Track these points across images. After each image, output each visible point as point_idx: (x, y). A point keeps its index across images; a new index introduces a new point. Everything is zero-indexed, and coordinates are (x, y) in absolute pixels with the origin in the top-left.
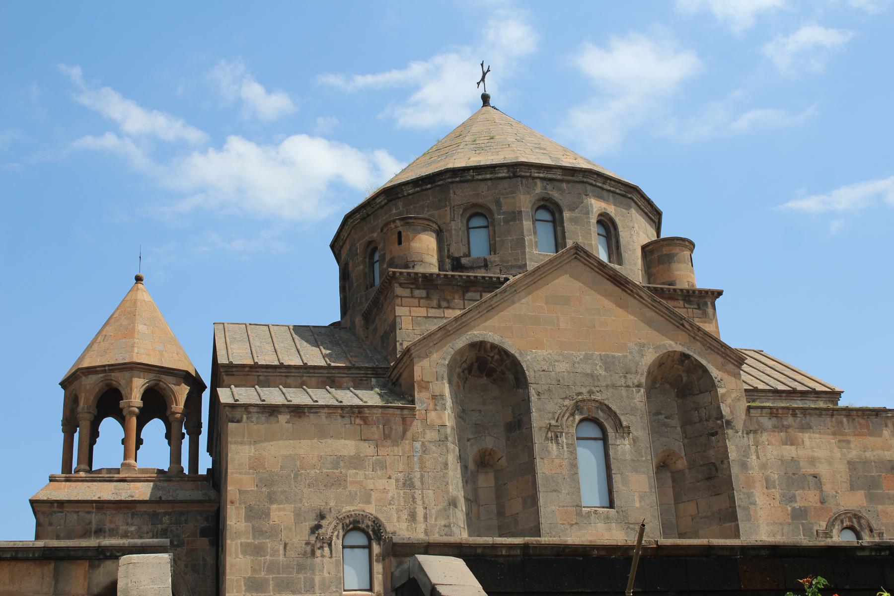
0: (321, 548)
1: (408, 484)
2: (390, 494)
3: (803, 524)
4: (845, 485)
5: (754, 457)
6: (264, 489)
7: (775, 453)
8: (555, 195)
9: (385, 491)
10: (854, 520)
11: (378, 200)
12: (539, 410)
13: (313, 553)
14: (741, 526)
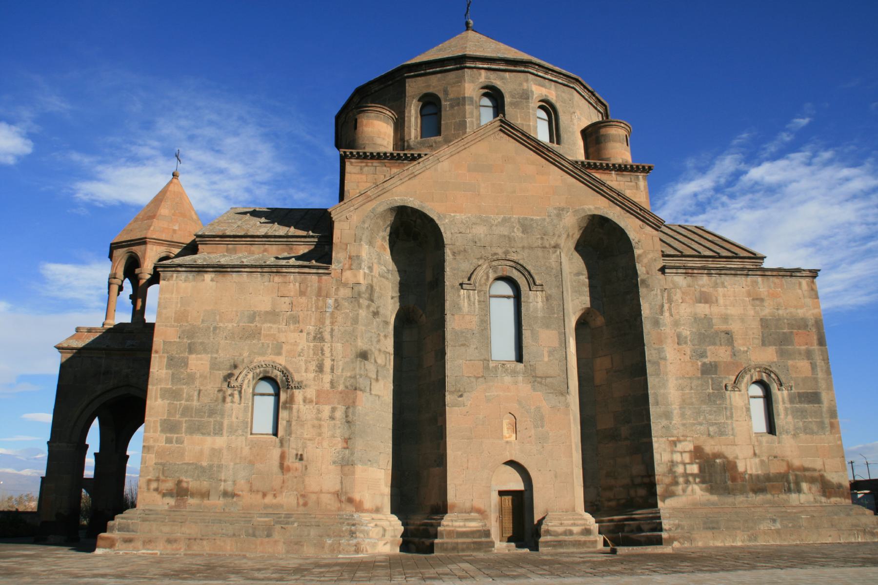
0: (232, 395)
1: (319, 337)
2: (299, 348)
4: (756, 341)
6: (185, 340)
7: (689, 310)
8: (498, 84)
9: (296, 344)
10: (764, 375)
11: (355, 100)
12: (453, 269)
13: (224, 400)
14: (651, 381)
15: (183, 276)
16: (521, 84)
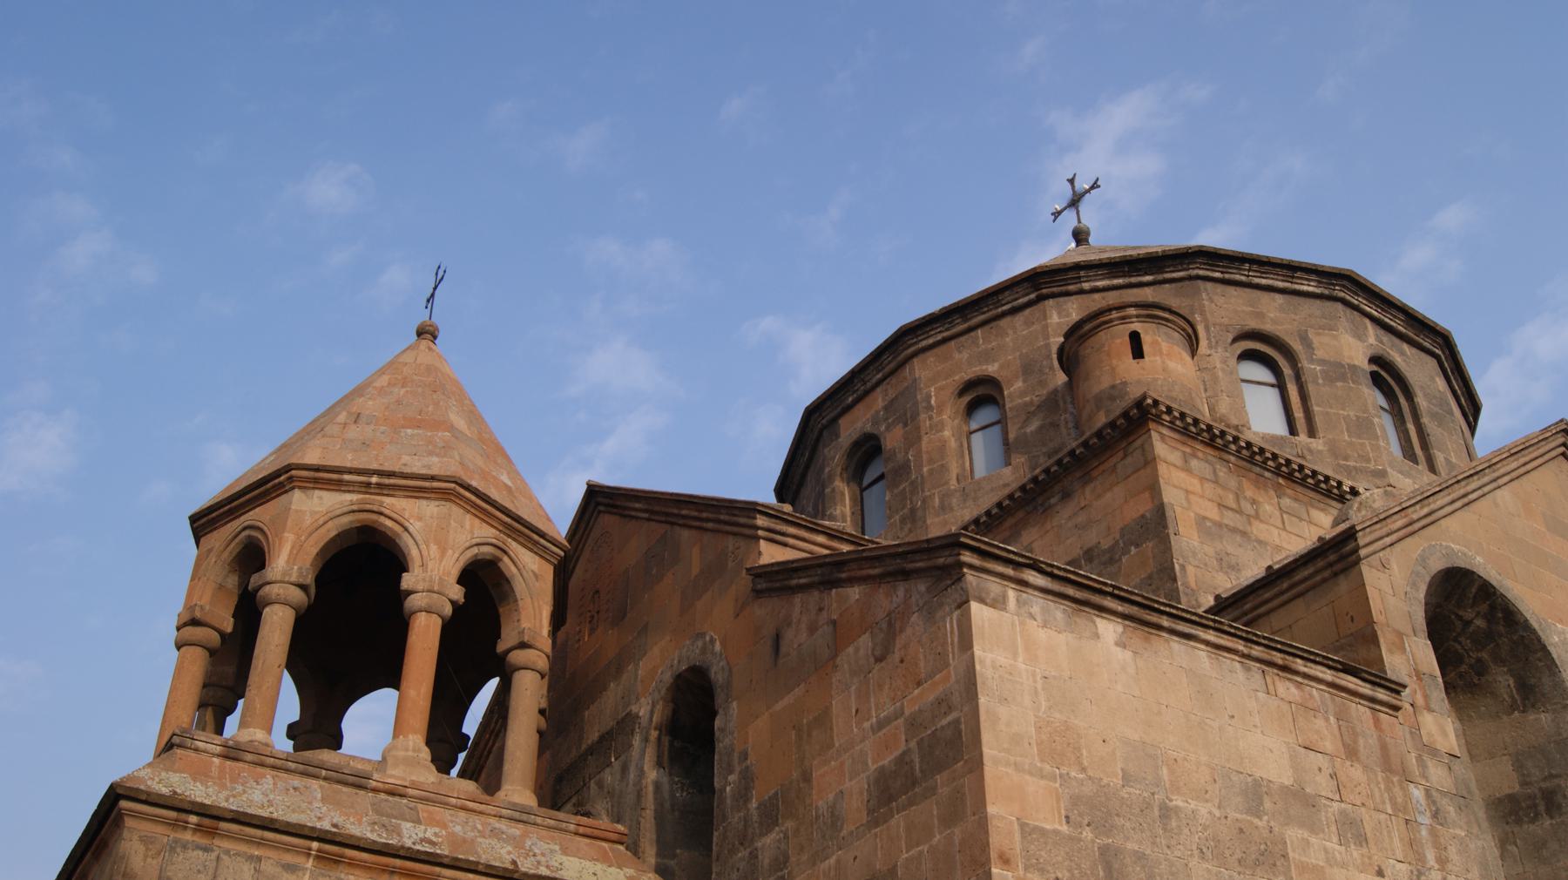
6: (1087, 834)
8: (1398, 360)
15: (1038, 603)
16: (1432, 379)
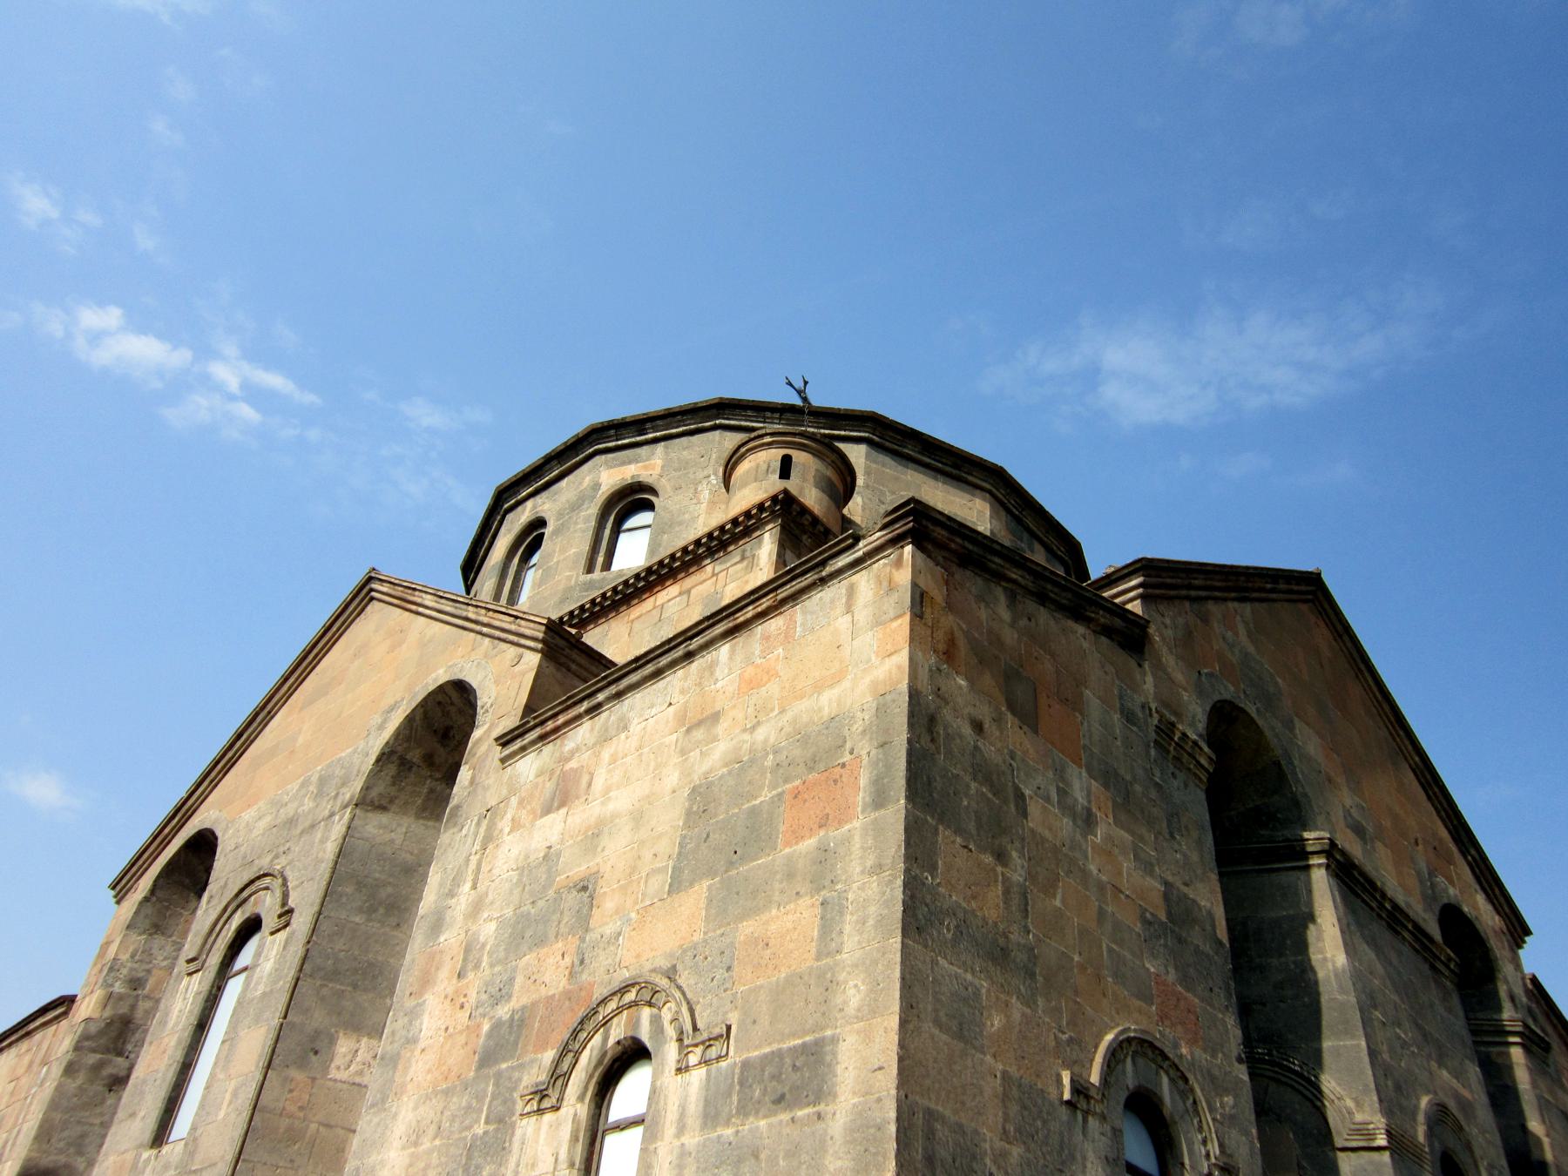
3: (499, 1075)
5: (467, 887)
7: (515, 852)
